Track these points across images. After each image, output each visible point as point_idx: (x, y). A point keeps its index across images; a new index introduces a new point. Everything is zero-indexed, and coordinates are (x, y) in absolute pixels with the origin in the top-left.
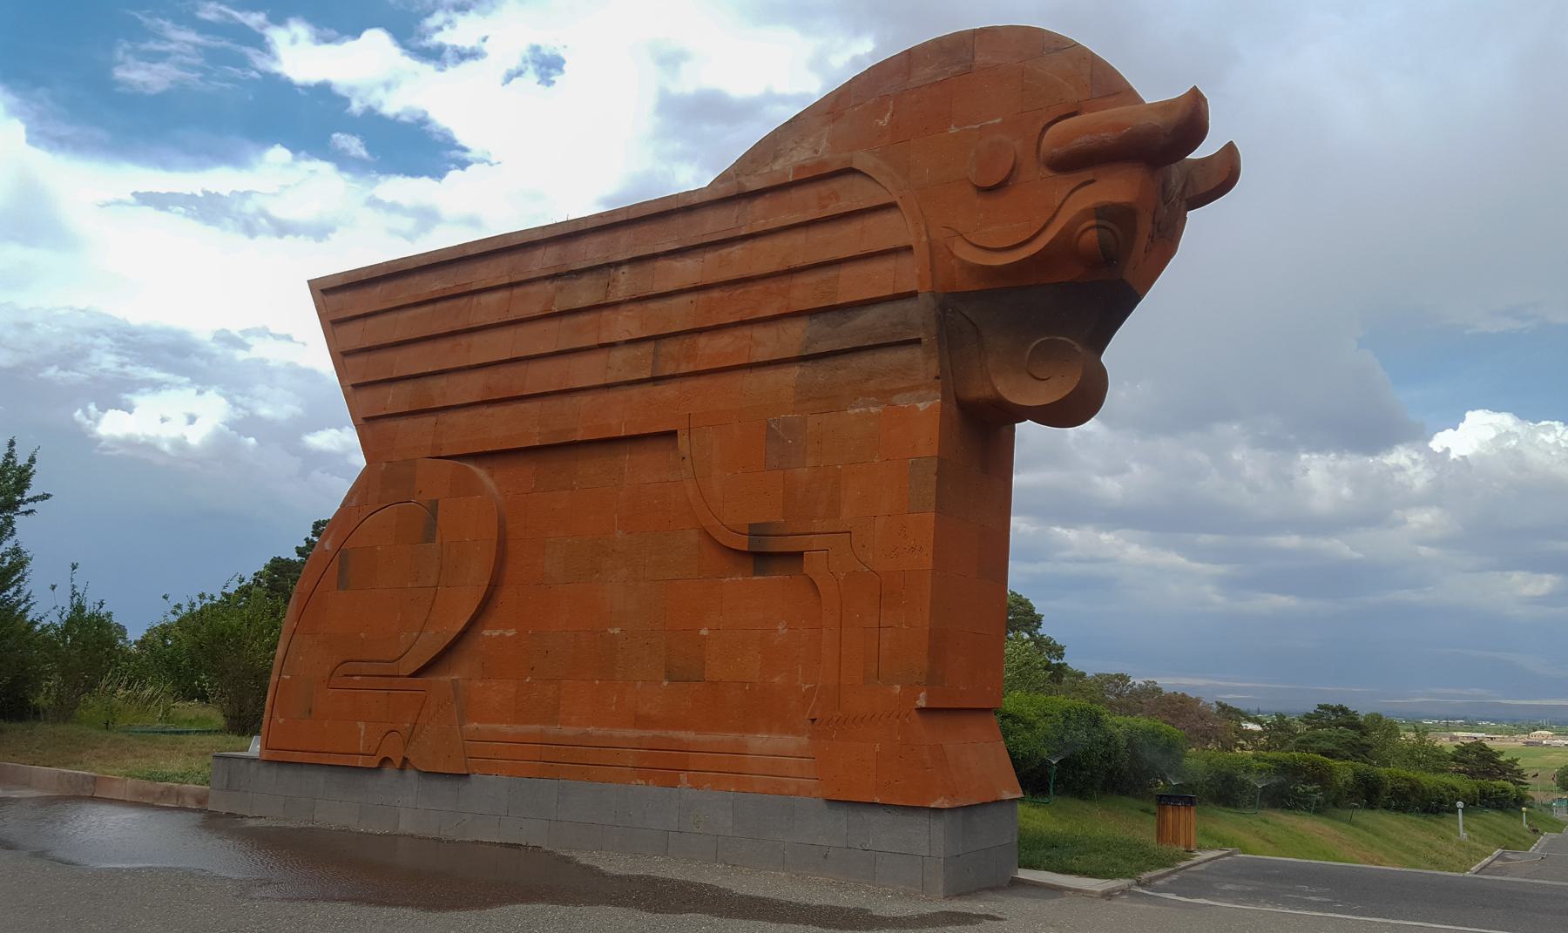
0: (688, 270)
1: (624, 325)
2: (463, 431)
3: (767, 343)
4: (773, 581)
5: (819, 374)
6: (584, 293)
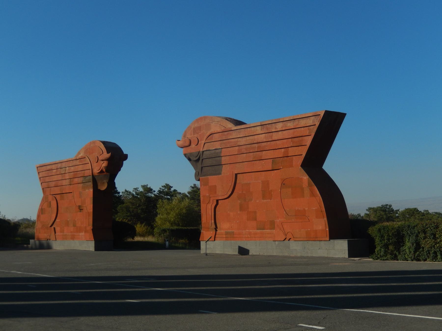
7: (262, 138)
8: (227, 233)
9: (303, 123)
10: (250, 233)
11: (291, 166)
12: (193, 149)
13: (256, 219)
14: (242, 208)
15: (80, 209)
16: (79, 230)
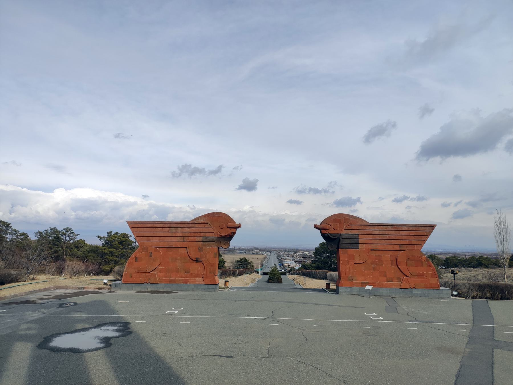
0: (188, 230)
1: (179, 235)
2: (155, 244)
3: (198, 239)
4: (199, 263)
5: (204, 243)
6: (174, 230)
7: (392, 232)
8: (362, 283)
9: (421, 229)
10: (383, 284)
11: (414, 250)
12: (331, 232)
13: (386, 276)
14: (374, 269)
15: (197, 261)
16: (197, 276)
